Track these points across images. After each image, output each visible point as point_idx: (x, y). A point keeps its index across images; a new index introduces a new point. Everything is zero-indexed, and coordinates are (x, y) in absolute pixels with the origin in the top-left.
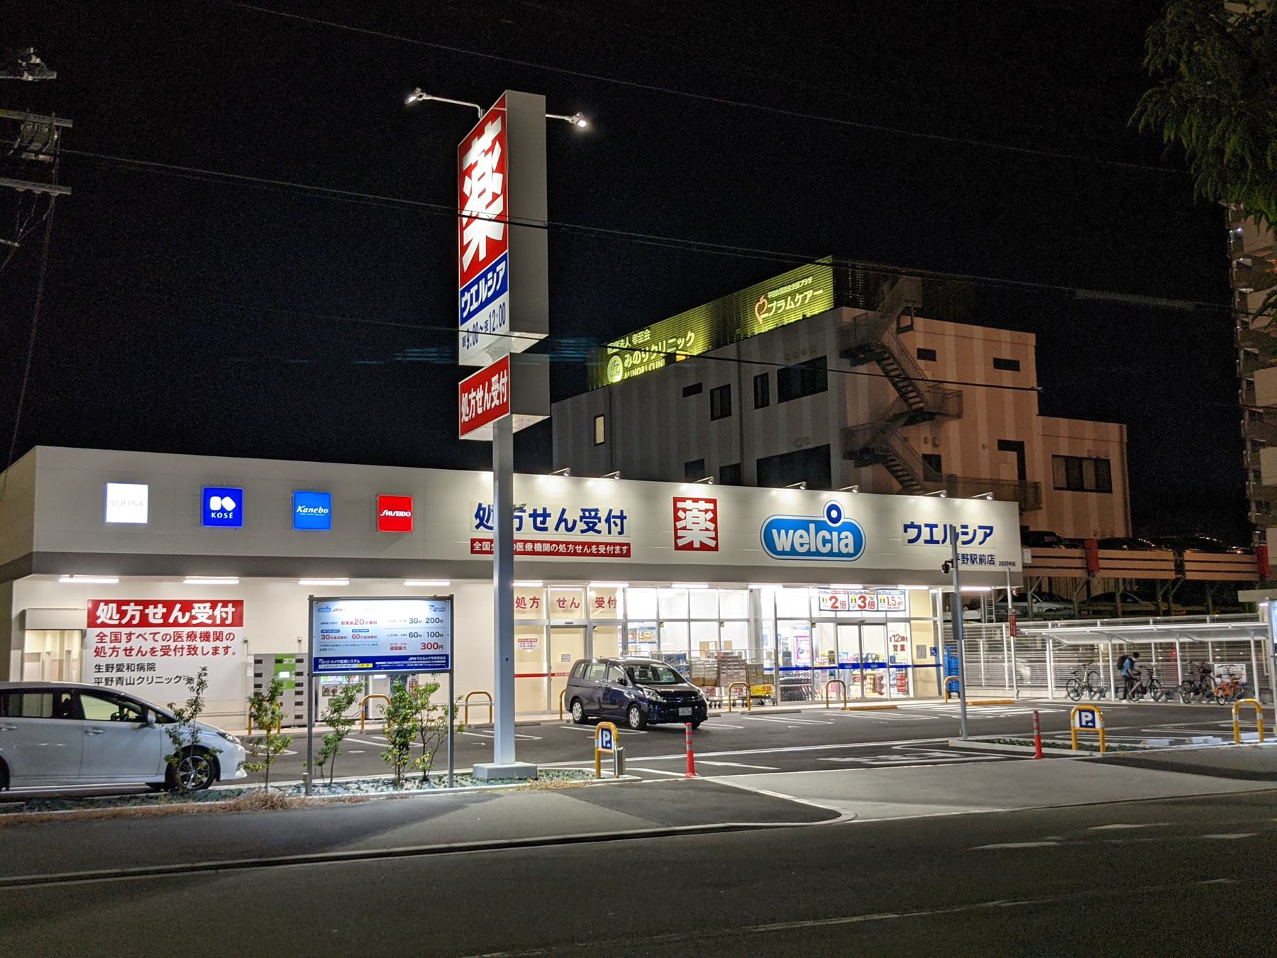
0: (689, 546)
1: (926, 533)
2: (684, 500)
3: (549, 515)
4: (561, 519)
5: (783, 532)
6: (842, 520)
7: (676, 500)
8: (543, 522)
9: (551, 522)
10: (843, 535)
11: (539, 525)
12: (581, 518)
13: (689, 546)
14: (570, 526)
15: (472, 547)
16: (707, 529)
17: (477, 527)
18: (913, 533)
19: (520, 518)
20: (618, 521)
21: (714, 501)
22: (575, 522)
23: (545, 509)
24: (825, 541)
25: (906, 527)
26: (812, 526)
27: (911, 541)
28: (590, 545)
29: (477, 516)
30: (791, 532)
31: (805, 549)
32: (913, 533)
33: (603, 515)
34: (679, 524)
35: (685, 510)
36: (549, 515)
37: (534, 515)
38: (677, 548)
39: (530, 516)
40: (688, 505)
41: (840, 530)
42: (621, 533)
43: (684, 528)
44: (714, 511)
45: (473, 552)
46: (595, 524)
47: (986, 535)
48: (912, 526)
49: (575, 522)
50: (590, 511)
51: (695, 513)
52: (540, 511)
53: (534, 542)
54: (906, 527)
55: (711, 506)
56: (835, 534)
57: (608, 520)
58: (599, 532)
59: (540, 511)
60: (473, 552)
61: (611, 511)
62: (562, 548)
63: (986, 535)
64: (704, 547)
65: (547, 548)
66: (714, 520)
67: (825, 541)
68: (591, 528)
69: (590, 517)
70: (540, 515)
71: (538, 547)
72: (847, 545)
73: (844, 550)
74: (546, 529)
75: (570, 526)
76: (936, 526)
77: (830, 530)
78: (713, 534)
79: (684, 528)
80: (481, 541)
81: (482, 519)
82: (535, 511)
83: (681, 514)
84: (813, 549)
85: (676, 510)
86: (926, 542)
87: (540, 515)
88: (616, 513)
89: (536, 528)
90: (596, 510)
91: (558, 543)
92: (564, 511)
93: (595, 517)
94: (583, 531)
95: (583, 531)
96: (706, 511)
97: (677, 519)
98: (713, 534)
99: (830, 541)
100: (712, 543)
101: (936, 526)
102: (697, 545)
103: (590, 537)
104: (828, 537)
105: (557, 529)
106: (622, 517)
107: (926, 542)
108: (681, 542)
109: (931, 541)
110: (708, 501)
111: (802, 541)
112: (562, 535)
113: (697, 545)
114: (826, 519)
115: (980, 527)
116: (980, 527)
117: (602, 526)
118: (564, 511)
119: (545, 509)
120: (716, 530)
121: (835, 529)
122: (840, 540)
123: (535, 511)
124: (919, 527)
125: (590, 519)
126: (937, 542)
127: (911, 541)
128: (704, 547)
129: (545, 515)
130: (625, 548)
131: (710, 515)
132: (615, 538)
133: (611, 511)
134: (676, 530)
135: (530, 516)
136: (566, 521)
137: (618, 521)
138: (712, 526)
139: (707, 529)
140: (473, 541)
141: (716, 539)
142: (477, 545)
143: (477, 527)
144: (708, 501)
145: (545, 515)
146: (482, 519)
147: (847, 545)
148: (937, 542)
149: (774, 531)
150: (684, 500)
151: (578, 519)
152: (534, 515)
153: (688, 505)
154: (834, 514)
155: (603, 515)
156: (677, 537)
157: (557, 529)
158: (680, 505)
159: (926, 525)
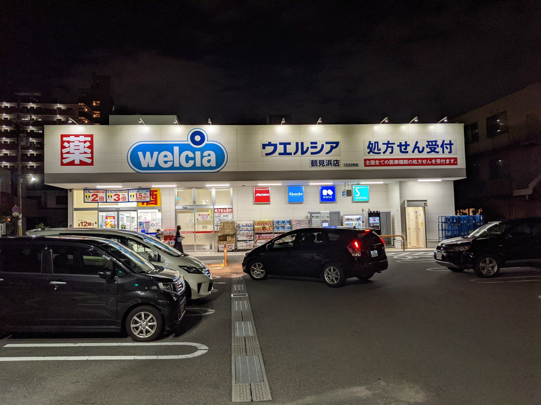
0: (72, 163)
1: (280, 149)
2: (68, 136)
3: (409, 145)
4: (416, 147)
5: (148, 154)
6: (206, 142)
7: (62, 136)
8: (406, 149)
9: (410, 149)
10: (206, 153)
11: (403, 150)
12: (427, 146)
13: (72, 163)
14: (421, 150)
15: (365, 163)
16: (85, 153)
17: (369, 153)
18: (270, 149)
19: (392, 147)
20: (448, 146)
21: (91, 136)
22: (423, 148)
23: (406, 142)
24: (188, 159)
25: (264, 146)
26: (176, 149)
27: (267, 154)
28: (431, 159)
29: (369, 147)
30: (156, 153)
31: (169, 165)
32: (270, 149)
33: (439, 143)
34: (64, 151)
35: (68, 142)
36: (409, 145)
37: (400, 145)
38: (62, 164)
39: (398, 146)
40: (72, 139)
41: (202, 150)
42: (391, 153)
43: (68, 153)
44: (91, 142)
45: (365, 166)
46: (435, 148)
47: (332, 148)
48: (270, 144)
49: (423, 148)
50: (432, 142)
51: (77, 143)
52: (403, 143)
53: (398, 159)
54: (264, 146)
55: (89, 139)
56: (198, 153)
57: (442, 146)
58: (438, 152)
59: (403, 143)
60: (365, 166)
61: (444, 141)
62: (415, 162)
63: (332, 148)
64: (82, 163)
65: (406, 162)
66: (91, 147)
67: (188, 159)
68: (433, 150)
69: (432, 145)
70: (403, 145)
71: (401, 162)
72: (209, 161)
73: (206, 164)
74: (407, 152)
75: (421, 150)
76: (290, 144)
77: (194, 151)
78: (90, 156)
79: (68, 153)
80: (369, 160)
81: (371, 149)
82: (401, 143)
83: (66, 144)
84: (177, 165)
85: (62, 142)
86: (280, 154)
87: (403, 145)
88: (447, 142)
89: (401, 151)
90: (436, 141)
91: (412, 159)
92: (417, 143)
93: (436, 145)
94: (428, 153)
95: (428, 153)
96: (85, 142)
97: (63, 147)
98: (90, 156)
99: (194, 159)
100: (89, 161)
101: (290, 144)
102: (77, 162)
103: (433, 155)
104: (191, 155)
105: (413, 152)
106: (451, 144)
107: (280, 154)
108: (65, 161)
109: (285, 153)
110: (86, 136)
111: (166, 159)
112: (417, 155)
113: (77, 162)
114: (190, 142)
115: (327, 143)
116: (327, 143)
117: (439, 149)
118: (417, 143)
119: (406, 142)
120: (92, 153)
121: (198, 150)
122: (202, 157)
123: (401, 143)
124: (275, 146)
125: (432, 146)
126: (290, 154)
127: (267, 154)
128: (82, 163)
129: (407, 145)
130: (452, 160)
131: (88, 144)
132: (447, 155)
133: (444, 141)
134: (62, 154)
135: (398, 146)
136: (418, 148)
137: (448, 146)
138: (89, 151)
139: (85, 153)
140: (365, 160)
141: (92, 158)
142: (368, 162)
143: (369, 153)
144: (86, 136)
145: (407, 145)
146: (371, 149)
147: (209, 161)
148: (290, 154)
149: (140, 154)
150: (68, 136)
151: (425, 147)
152: (400, 145)
153: (72, 139)
154: (198, 138)
155: (439, 143)
156: (62, 158)
157: (413, 152)
158: (65, 139)
159: (281, 144)
